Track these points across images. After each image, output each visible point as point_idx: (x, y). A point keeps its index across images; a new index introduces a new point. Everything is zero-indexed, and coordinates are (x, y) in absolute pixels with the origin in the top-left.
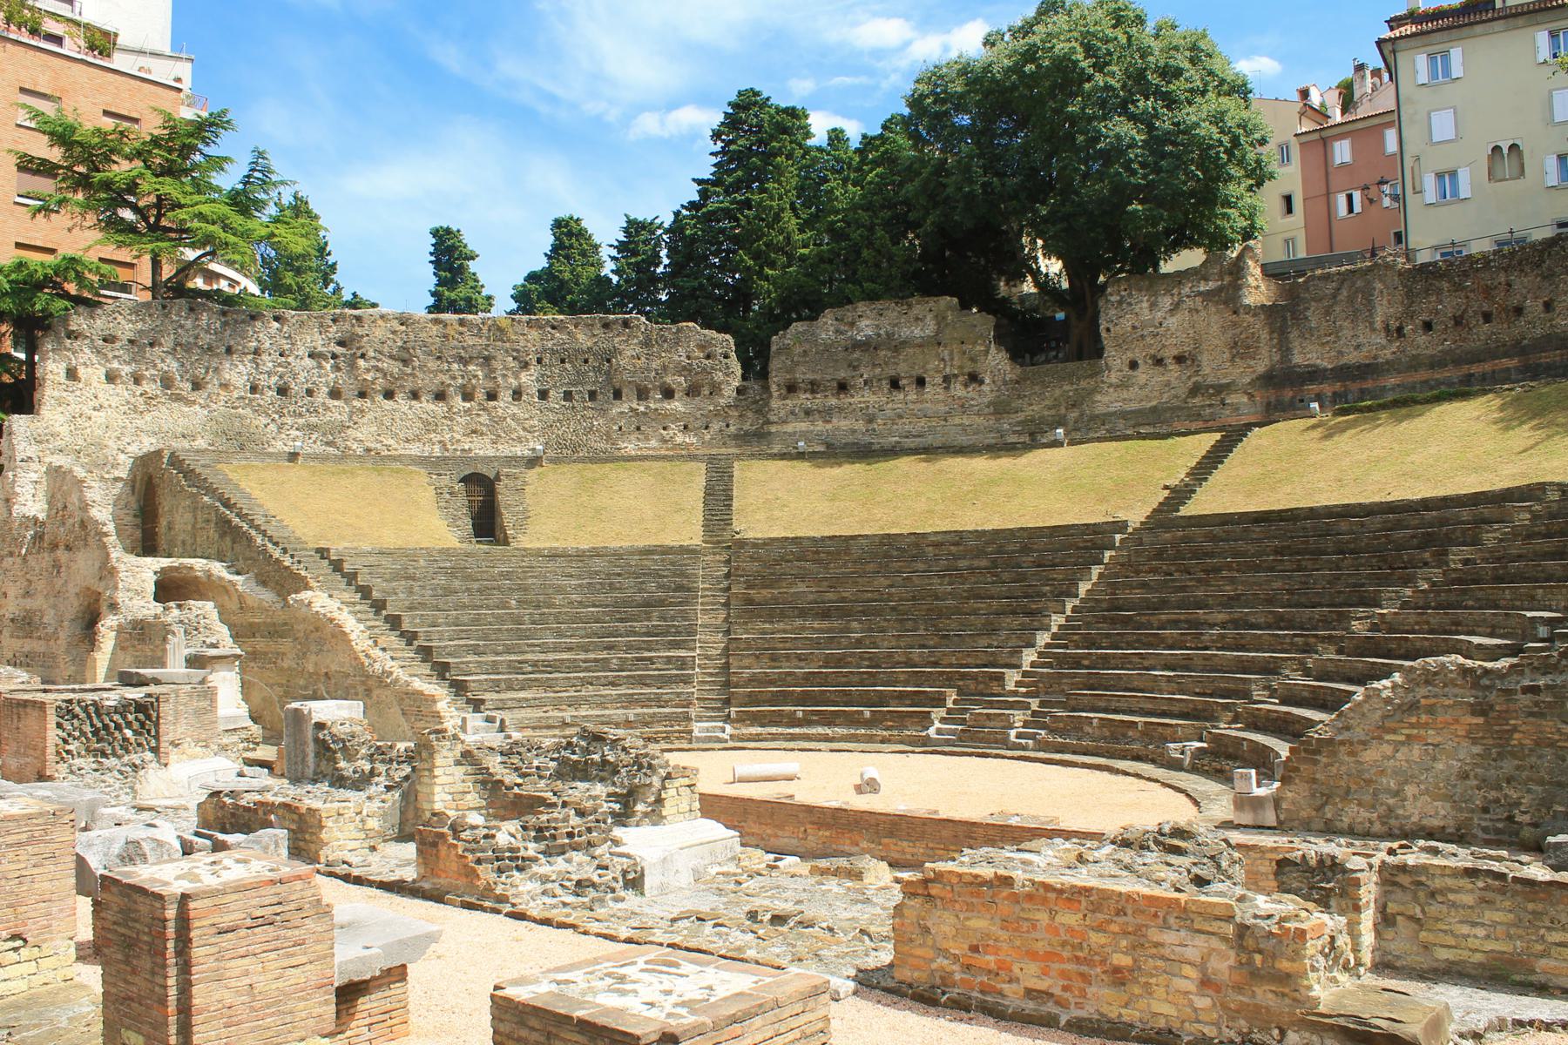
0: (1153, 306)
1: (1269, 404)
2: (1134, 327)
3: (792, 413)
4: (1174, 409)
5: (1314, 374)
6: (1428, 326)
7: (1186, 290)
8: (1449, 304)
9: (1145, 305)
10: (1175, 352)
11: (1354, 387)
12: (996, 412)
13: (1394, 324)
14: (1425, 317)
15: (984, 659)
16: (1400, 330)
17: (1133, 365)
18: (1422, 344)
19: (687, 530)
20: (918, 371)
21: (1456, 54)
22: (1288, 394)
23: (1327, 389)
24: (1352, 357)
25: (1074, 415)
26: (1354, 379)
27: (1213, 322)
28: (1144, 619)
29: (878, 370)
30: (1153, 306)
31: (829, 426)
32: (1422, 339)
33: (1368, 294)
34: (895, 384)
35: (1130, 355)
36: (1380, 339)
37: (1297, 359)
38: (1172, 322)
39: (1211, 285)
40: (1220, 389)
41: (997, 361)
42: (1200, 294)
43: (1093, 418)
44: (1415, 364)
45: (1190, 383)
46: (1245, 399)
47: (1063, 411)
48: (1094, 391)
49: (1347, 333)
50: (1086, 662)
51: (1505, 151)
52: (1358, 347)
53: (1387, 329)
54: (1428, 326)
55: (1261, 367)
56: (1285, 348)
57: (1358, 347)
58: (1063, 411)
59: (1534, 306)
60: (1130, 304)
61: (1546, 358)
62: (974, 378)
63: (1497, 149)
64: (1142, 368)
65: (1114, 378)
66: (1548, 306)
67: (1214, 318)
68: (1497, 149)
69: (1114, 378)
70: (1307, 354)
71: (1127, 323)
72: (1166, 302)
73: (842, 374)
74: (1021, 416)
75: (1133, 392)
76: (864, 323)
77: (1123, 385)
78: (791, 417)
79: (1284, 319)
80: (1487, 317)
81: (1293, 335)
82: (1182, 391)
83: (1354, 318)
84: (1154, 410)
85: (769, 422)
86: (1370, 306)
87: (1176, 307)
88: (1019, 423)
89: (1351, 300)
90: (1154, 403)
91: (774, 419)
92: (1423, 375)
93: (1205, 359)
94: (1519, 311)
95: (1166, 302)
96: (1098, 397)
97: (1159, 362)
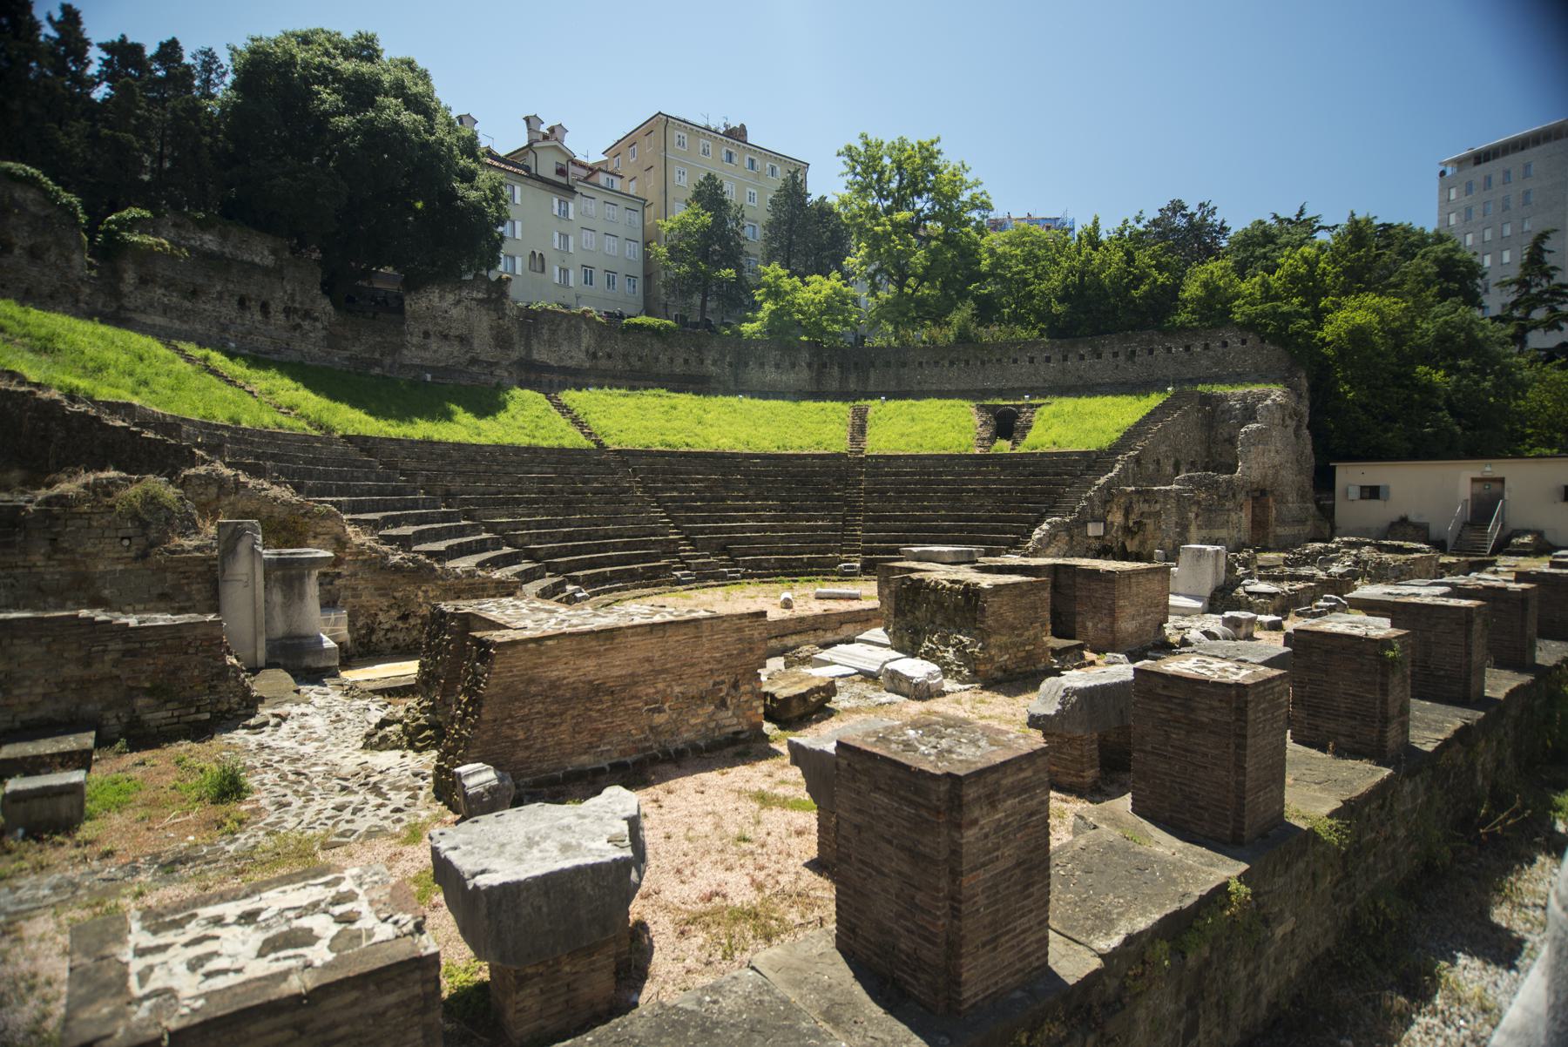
0: (441, 298)
3: (151, 305)
5: (546, 368)
6: (609, 356)
7: (464, 294)
8: (620, 347)
12: (329, 346)
13: (591, 350)
17: (426, 335)
18: (603, 363)
21: (518, 189)
25: (388, 361)
29: (231, 286)
30: (441, 298)
31: (185, 327)
33: (578, 328)
34: (242, 303)
35: (423, 328)
36: (582, 356)
37: (536, 356)
38: (454, 312)
39: (480, 296)
41: (325, 305)
43: (402, 366)
47: (377, 356)
48: (403, 346)
49: (565, 348)
54: (609, 356)
55: (516, 354)
58: (377, 356)
59: (664, 358)
62: (307, 315)
64: (433, 338)
65: (415, 340)
66: (672, 360)
69: (415, 340)
70: (541, 354)
71: (424, 304)
73: (200, 281)
74: (347, 354)
75: (427, 355)
76: (207, 237)
77: (424, 347)
78: (150, 310)
85: (121, 307)
88: (349, 359)
89: (568, 331)
91: (131, 306)
94: (657, 359)
95: (450, 298)
96: (405, 352)
97: (446, 337)
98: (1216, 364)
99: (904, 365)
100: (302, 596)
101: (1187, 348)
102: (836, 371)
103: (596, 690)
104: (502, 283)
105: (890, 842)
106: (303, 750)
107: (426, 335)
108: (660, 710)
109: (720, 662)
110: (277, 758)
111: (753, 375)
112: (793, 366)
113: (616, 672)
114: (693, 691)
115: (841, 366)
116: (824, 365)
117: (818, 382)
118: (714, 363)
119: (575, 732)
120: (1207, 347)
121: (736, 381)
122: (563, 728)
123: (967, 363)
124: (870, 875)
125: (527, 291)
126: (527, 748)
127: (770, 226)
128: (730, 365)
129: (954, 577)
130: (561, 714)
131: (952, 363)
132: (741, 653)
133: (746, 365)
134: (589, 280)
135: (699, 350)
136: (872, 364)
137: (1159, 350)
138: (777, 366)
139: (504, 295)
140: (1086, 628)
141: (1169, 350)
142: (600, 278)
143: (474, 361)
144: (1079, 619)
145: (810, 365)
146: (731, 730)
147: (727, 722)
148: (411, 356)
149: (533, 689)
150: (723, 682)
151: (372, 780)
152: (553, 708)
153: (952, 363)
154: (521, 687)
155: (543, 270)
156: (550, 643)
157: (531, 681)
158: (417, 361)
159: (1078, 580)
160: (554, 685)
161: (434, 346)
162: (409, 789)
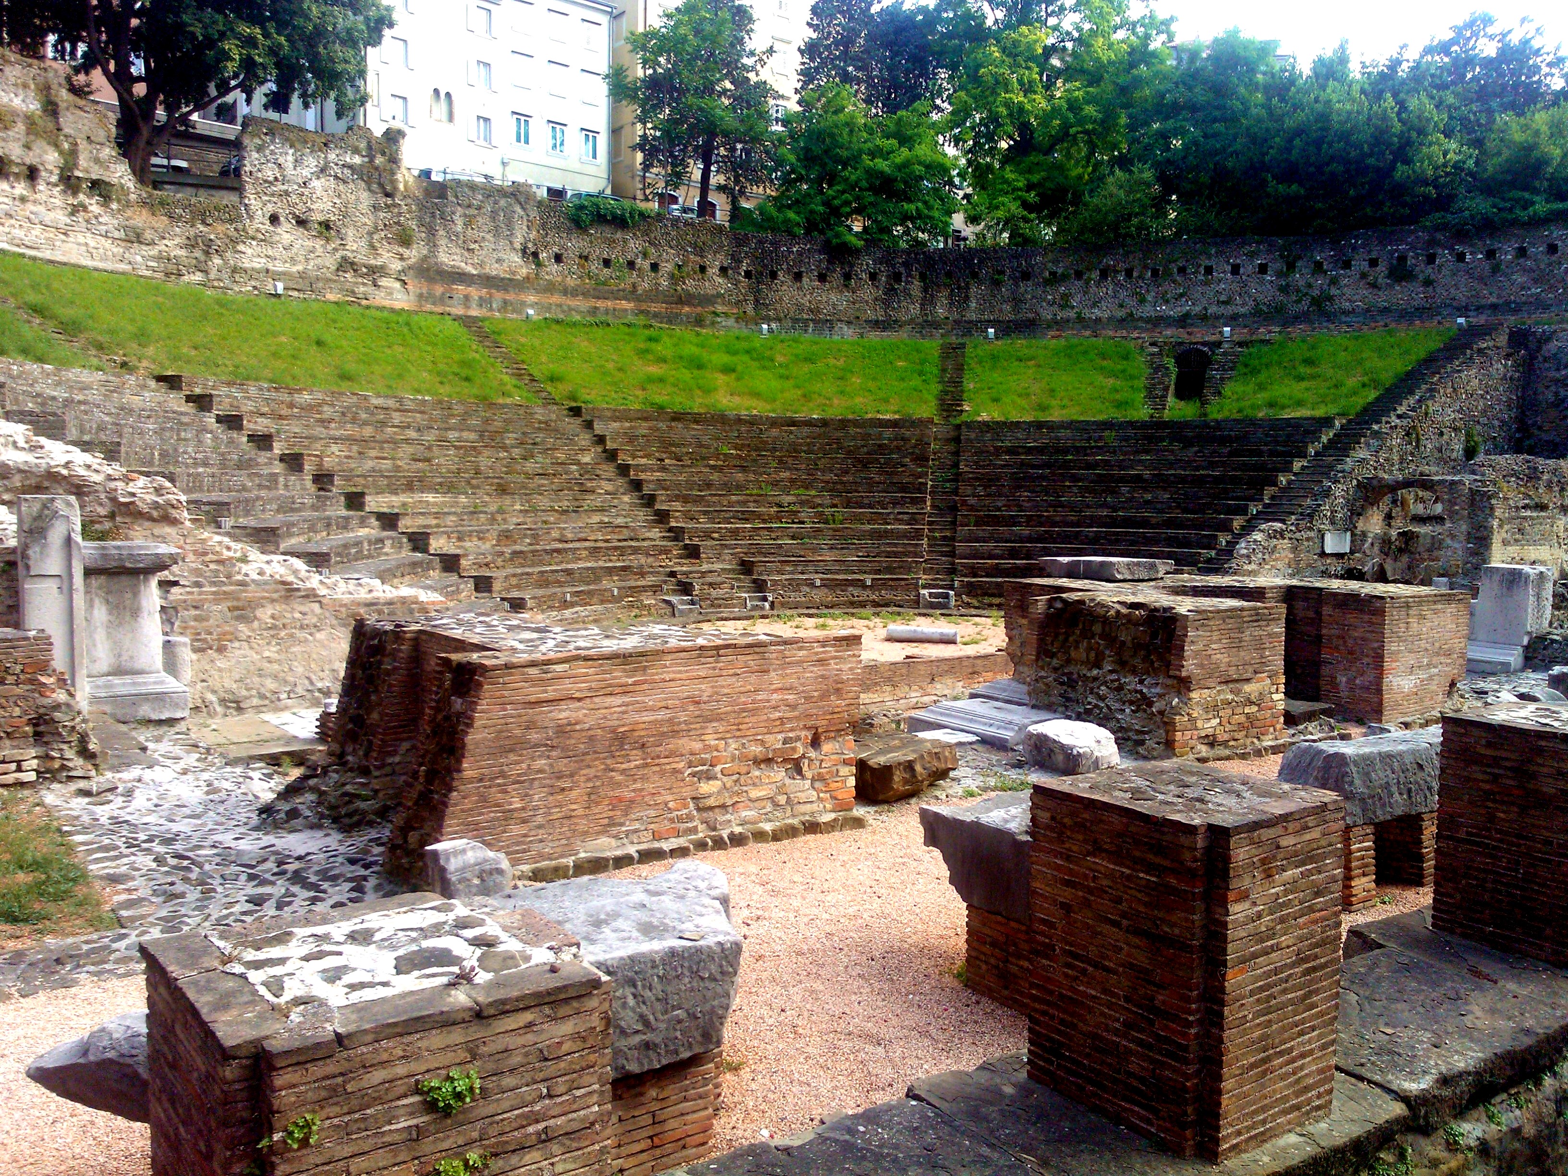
0: (297, 162)
1: (421, 296)
2: (276, 179)
4: (329, 280)
5: (461, 277)
6: (558, 258)
7: (332, 156)
9: (290, 158)
10: (320, 218)
11: (499, 296)
14: (556, 249)
15: (626, 533)
16: (535, 255)
17: (274, 219)
19: (925, 408)
20: (30, 159)
22: (439, 290)
23: (475, 292)
24: (494, 269)
26: (498, 288)
27: (362, 198)
28: (715, 499)
32: (555, 268)
35: (270, 208)
36: (516, 259)
38: (316, 183)
39: (357, 160)
40: (375, 272)
42: (350, 167)
44: (550, 288)
45: (338, 255)
46: (397, 285)
50: (716, 535)
51: (442, 95)
52: (499, 261)
53: (524, 251)
56: (433, 245)
57: (499, 261)
60: (273, 153)
61: (654, 308)
63: (436, 91)
67: (364, 195)
68: (436, 91)
72: (311, 163)
79: (433, 215)
80: (607, 263)
81: (441, 233)
82: (331, 262)
83: (496, 232)
84: (302, 275)
86: (509, 225)
87: (323, 170)
88: (153, 258)
90: (300, 268)
92: (556, 299)
93: (350, 233)
95: (311, 163)
97: (301, 223)
98: (1536, 281)
99: (1026, 276)
100: (136, 612)
101: (1490, 254)
102: (916, 288)
103: (621, 740)
104: (393, 137)
105: (1116, 924)
106: (175, 827)
107: (274, 219)
108: (710, 777)
109: (793, 707)
110: (142, 836)
111: (787, 293)
112: (847, 277)
113: (648, 717)
114: (756, 750)
115: (923, 277)
116: (897, 277)
117: (887, 304)
118: (723, 270)
119: (590, 801)
120: (1522, 252)
121: (757, 301)
122: (574, 794)
123: (1129, 273)
124: (1084, 972)
125: (432, 151)
126: (524, 821)
127: (810, 50)
128: (748, 274)
129: (1131, 599)
130: (572, 775)
131: (1104, 275)
132: (824, 696)
133: (774, 275)
134: (523, 137)
135: (700, 251)
136: (975, 275)
137: (1445, 256)
138: (822, 278)
139: (394, 160)
140: (1335, 685)
141: (1461, 257)
142: (539, 132)
143: (346, 265)
144: (1325, 670)
145: (873, 277)
146: (808, 808)
147: (802, 796)
148: (251, 257)
149: (534, 736)
150: (798, 739)
151: (291, 867)
152: (562, 765)
153: (1104, 275)
154: (517, 732)
155: (451, 118)
156: (559, 668)
157: (530, 726)
158: (259, 263)
159: (1326, 610)
160: (563, 730)
161: (286, 238)
162: (350, 880)
